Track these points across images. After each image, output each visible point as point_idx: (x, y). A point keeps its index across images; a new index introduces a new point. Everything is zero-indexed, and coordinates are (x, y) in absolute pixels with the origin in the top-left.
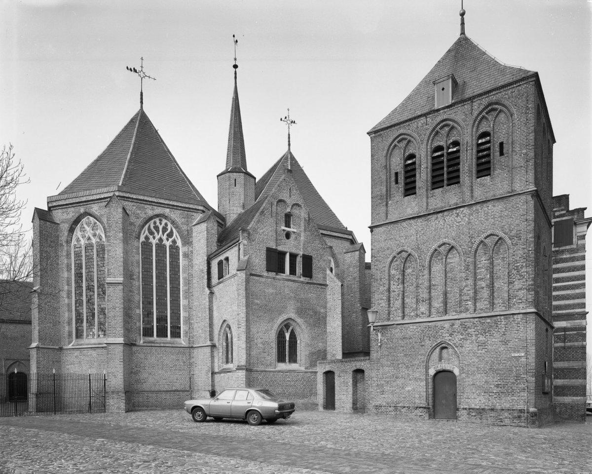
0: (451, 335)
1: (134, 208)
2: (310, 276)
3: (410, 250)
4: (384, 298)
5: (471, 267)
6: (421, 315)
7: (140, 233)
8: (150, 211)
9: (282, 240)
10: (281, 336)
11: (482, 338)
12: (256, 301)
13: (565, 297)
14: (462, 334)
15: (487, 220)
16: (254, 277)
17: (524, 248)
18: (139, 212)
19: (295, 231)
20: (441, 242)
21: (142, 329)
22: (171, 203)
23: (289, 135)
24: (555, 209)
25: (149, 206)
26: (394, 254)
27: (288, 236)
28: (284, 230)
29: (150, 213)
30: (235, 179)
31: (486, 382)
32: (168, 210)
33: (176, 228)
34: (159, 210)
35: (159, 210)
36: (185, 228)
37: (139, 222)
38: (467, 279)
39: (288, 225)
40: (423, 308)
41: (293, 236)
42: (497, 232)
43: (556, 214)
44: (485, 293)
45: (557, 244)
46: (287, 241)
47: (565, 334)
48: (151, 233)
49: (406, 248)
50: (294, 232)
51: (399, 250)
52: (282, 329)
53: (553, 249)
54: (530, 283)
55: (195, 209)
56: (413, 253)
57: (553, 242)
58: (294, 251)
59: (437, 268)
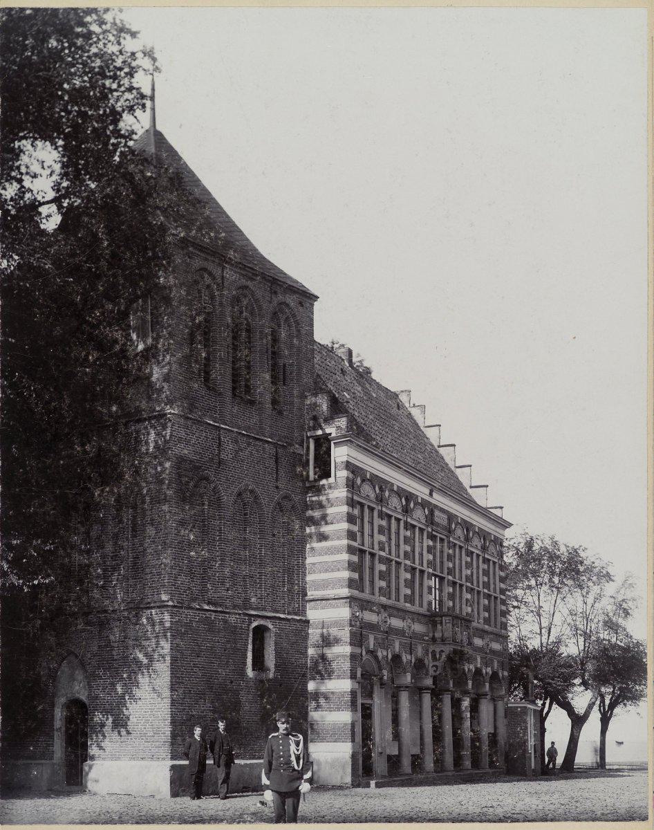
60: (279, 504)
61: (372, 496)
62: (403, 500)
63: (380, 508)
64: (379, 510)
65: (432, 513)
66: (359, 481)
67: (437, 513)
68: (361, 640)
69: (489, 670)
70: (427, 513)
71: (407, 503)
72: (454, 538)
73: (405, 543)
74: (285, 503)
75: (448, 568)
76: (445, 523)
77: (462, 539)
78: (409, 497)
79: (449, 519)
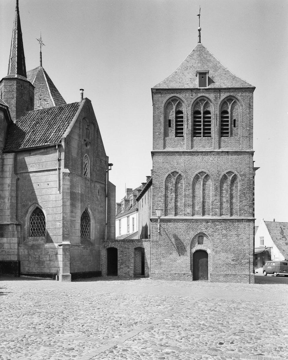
0: (206, 229)
3: (180, 172)
4: (162, 200)
5: (219, 189)
6: (187, 215)
11: (224, 232)
14: (213, 229)
15: (228, 163)
17: (248, 183)
20: (200, 171)
23: (41, 53)
26: (170, 172)
31: (227, 258)
38: (216, 196)
40: (189, 210)
42: (233, 171)
44: (226, 205)
49: (177, 170)
51: (173, 171)
54: (251, 203)
56: (182, 174)
59: (199, 187)
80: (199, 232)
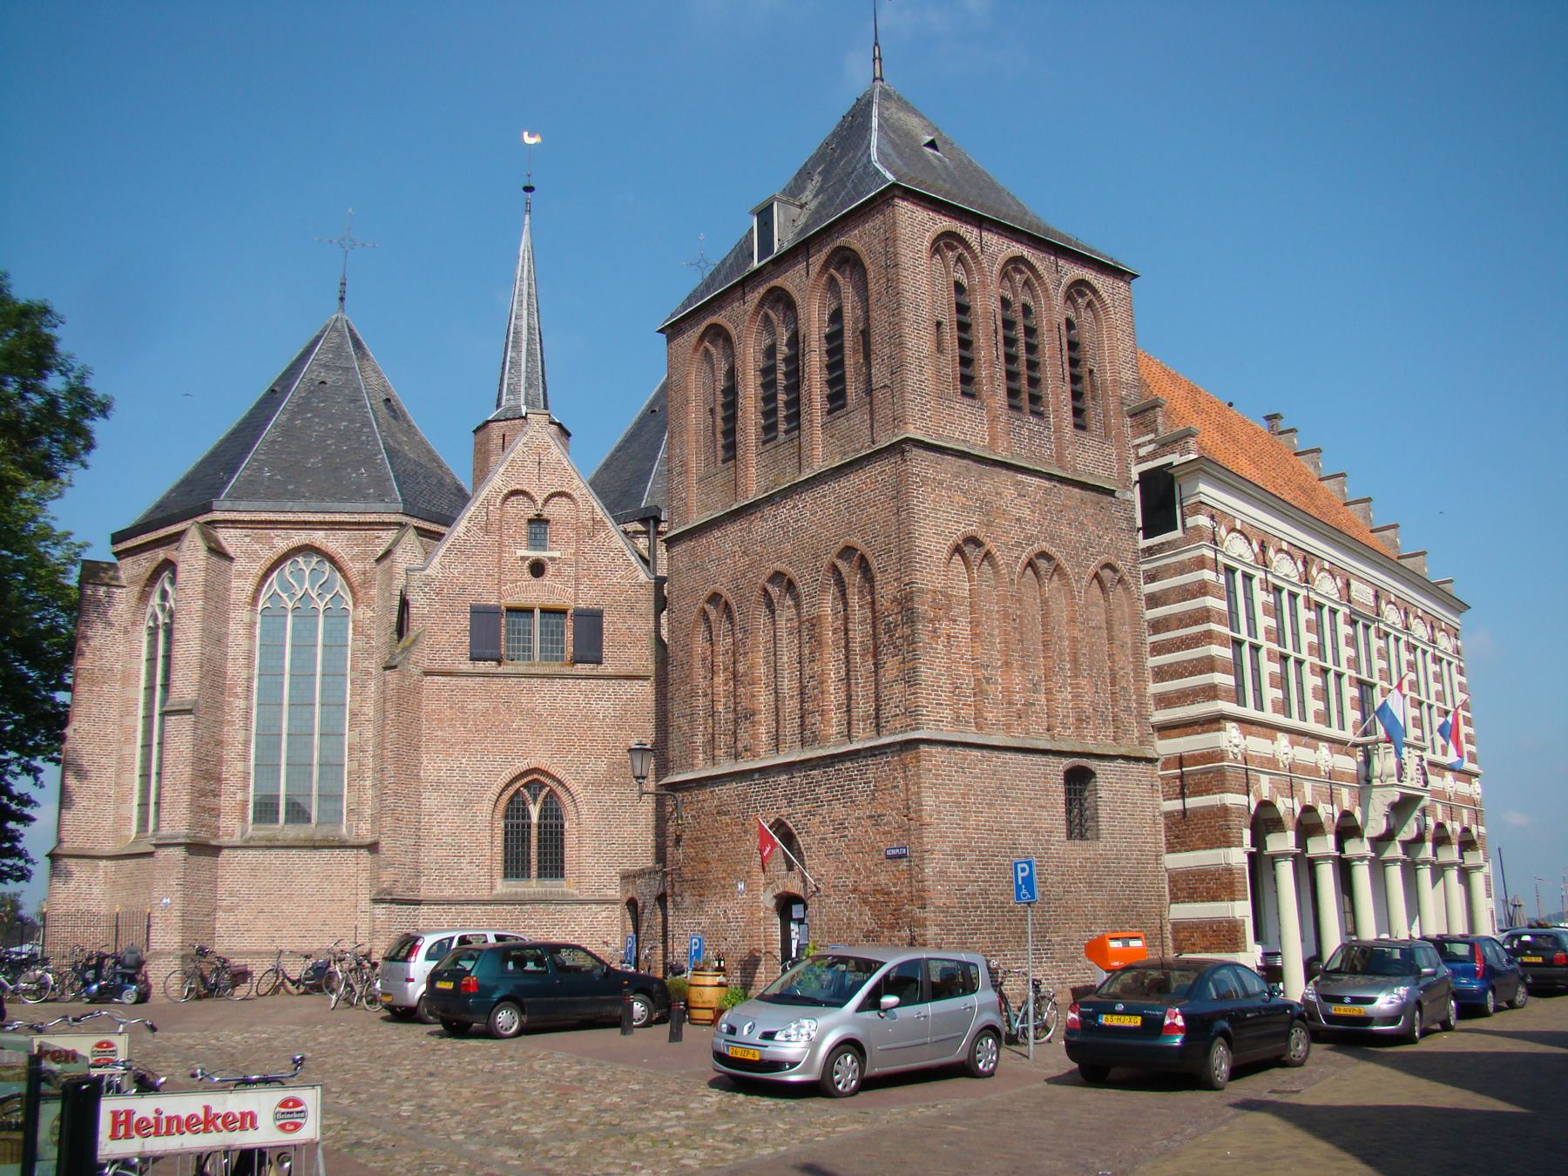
1: (247, 539)
2: (598, 661)
7: (258, 591)
8: (284, 541)
9: (517, 581)
10: (515, 810)
12: (440, 733)
13: (1166, 672)
16: (436, 678)
18: (257, 547)
19: (556, 554)
21: (251, 805)
22: (328, 518)
24: (1137, 441)
25: (279, 532)
27: (537, 569)
28: (523, 559)
29: (284, 541)
30: (504, 436)
32: (321, 533)
33: (340, 570)
34: (300, 538)
35: (300, 538)
36: (354, 568)
37: (258, 568)
39: (536, 541)
41: (550, 569)
43: (1143, 452)
45: (1149, 532)
46: (534, 581)
47: (1181, 777)
48: (287, 587)
50: (552, 559)
52: (518, 791)
53: (1144, 543)
55: (384, 523)
57: (1139, 524)
58: (554, 602)
60: (1096, 576)
61: (1249, 558)
62: (1299, 564)
63: (1262, 575)
64: (1261, 579)
65: (1348, 585)
66: (1223, 531)
67: (1354, 584)
68: (1247, 786)
69: (1457, 827)
70: (1340, 585)
71: (1306, 570)
72: (1387, 625)
73: (1309, 629)
74: (1106, 574)
75: (1380, 671)
76: (1371, 601)
77: (1399, 626)
78: (1308, 559)
79: (1377, 597)
80: (773, 820)
